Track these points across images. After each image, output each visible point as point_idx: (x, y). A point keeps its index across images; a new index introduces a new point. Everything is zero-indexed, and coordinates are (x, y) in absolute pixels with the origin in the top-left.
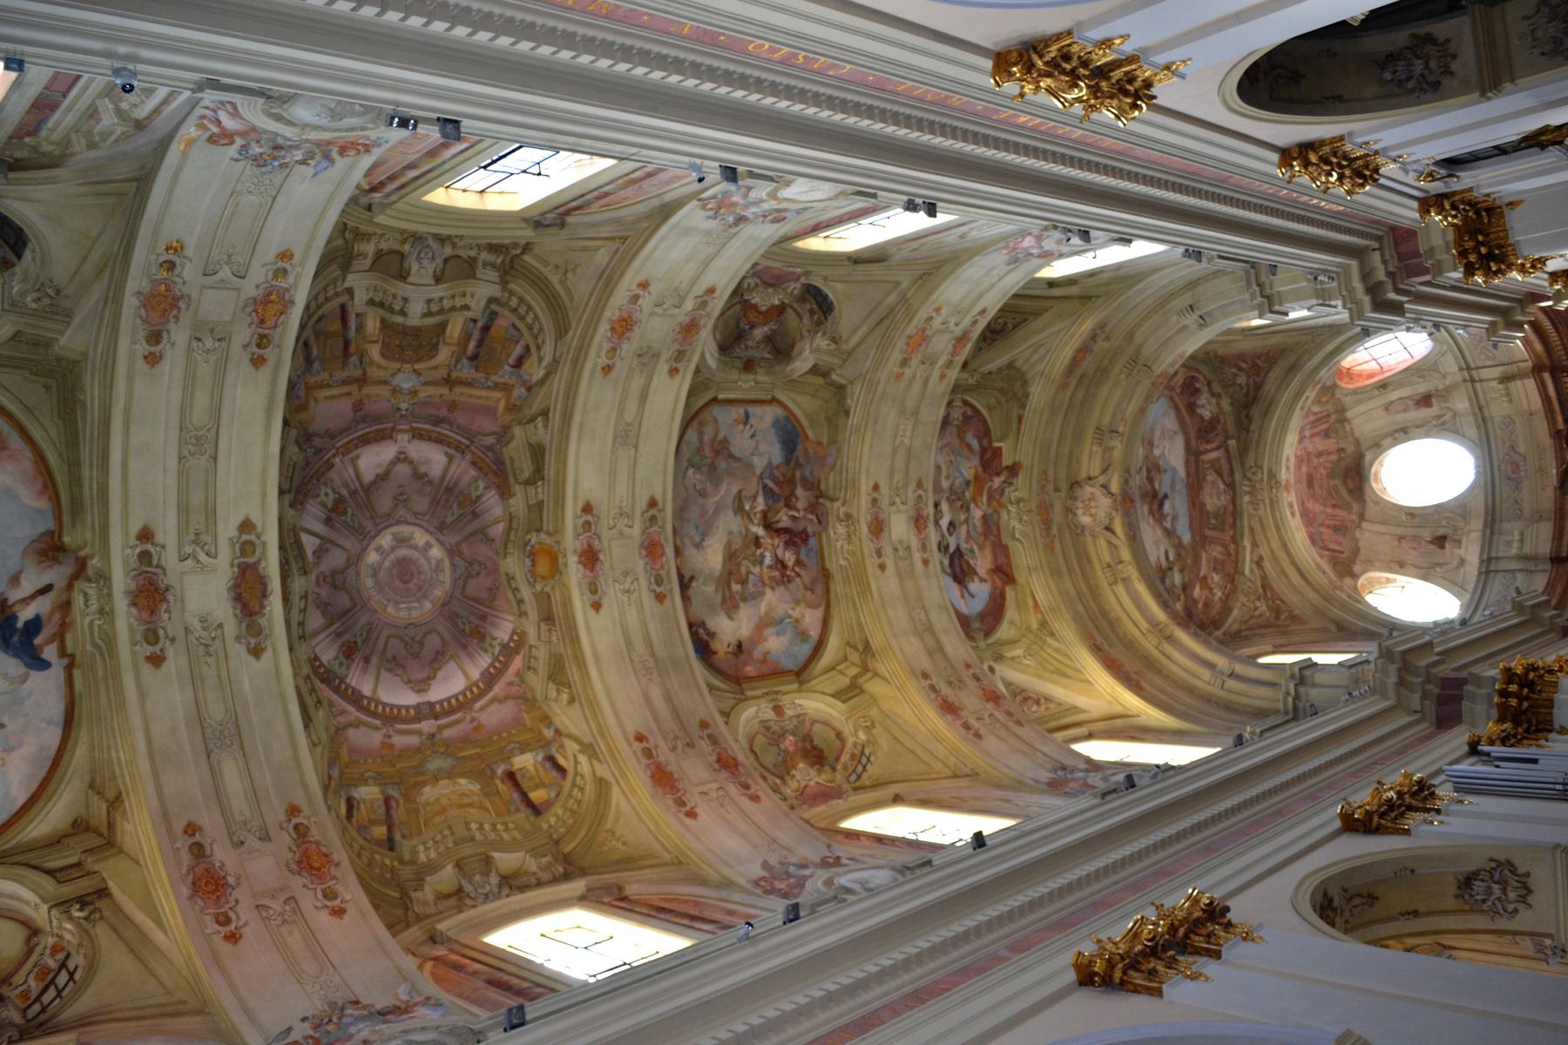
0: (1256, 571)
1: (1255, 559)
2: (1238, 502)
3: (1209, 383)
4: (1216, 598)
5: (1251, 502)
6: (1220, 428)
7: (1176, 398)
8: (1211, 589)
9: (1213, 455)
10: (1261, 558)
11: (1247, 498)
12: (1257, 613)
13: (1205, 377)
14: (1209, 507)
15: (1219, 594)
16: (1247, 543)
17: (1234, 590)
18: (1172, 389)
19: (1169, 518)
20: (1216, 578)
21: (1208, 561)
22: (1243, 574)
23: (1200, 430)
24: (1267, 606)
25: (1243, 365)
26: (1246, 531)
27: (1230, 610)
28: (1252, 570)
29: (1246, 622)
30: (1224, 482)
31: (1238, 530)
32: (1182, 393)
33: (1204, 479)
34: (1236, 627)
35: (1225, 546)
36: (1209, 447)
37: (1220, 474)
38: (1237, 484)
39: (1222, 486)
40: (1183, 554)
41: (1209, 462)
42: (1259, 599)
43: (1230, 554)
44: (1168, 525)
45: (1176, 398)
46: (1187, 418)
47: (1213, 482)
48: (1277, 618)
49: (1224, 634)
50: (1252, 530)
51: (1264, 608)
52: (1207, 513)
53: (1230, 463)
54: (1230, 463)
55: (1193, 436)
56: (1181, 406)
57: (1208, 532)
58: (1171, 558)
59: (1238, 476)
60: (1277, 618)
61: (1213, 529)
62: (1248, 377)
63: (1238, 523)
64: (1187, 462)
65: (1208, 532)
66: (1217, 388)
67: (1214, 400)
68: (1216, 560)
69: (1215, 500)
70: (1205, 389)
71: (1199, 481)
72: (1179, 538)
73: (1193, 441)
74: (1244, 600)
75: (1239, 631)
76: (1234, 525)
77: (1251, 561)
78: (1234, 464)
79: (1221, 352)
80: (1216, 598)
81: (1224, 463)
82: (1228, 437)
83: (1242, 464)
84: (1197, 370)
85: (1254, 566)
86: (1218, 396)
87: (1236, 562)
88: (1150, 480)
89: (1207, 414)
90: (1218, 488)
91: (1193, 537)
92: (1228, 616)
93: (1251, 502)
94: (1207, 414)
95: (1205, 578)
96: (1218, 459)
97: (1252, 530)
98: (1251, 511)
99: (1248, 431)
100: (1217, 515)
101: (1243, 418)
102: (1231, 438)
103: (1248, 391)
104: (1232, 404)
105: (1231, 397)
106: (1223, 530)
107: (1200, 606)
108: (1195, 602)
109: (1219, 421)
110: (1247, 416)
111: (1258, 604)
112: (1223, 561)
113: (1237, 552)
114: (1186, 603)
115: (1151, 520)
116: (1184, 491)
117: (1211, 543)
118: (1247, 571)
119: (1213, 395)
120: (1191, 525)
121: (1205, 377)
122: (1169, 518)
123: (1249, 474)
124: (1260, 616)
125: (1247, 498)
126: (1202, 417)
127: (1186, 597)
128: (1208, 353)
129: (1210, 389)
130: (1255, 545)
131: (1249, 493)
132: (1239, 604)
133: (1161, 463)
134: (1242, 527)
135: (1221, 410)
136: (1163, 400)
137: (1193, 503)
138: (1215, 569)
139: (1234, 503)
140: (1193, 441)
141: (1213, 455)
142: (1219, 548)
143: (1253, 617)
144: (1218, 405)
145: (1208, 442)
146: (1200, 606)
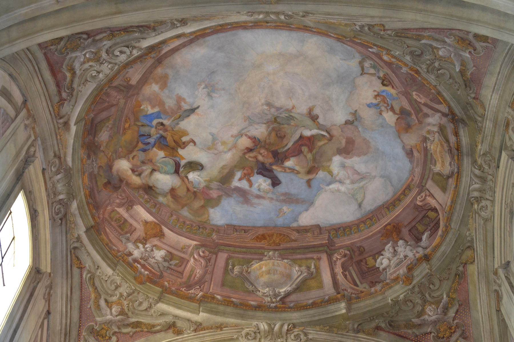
0: (161, 321)
1: (180, 324)
2: (259, 314)
3: (427, 258)
4: (130, 246)
5: (257, 331)
6: (363, 287)
7: (408, 200)
8: (144, 241)
9: (327, 278)
10: (179, 332)
11: (263, 326)
12: (102, 303)
13: (438, 246)
14: (256, 266)
15: (136, 254)
16: (202, 317)
17: (139, 280)
18: (422, 188)
19: (244, 184)
20: (159, 254)
21: (183, 249)
22: (160, 300)
23: (361, 250)
24: (110, 323)
25: (451, 313)
26: (219, 319)
27: (113, 266)
28: (163, 314)
29: (92, 279)
30: (288, 294)
31: (222, 308)
32: (417, 208)
33: (294, 261)
34: (88, 264)
35: (200, 282)
36: (339, 270)
37: (298, 289)
38: (285, 315)
39: (283, 290)
40: (197, 204)
41: (317, 268)
42: (122, 313)
43: (189, 287)
44: (236, 183)
45: (408, 200)
46: (378, 227)
47: (289, 276)
48: (92, 331)
49: (78, 239)
50: (220, 327)
51: (109, 317)
52: (248, 262)
53: (314, 305)
54: (314, 305)
55: (354, 239)
56: (398, 210)
57: (222, 257)
58: (192, 176)
59: (295, 316)
60: (92, 331)
61: (226, 270)
62: (435, 323)
63: (229, 309)
64: (317, 229)
65: (222, 257)
66: (423, 270)
67: (402, 271)
68: (183, 261)
69: (265, 279)
70: (421, 252)
71: (294, 250)
72: (215, 202)
73: (347, 241)
74: (124, 290)
75: (81, 268)
76: (228, 302)
77: (176, 316)
78: (312, 312)
79: (472, 269)
80: (130, 246)
81: (313, 295)
82: (349, 301)
83: (312, 324)
84: (444, 237)
85: (169, 319)
86: (408, 278)
87: (177, 294)
88: (296, 151)
89: (383, 262)
90: (281, 285)
91: (217, 229)
92: (105, 257)
93: (257, 331)
94: (383, 262)
95: (161, 235)
96: (321, 286)
97: (220, 327)
98: (246, 330)
99: (357, 331)
100: (244, 277)
101: (373, 325)
102: (349, 308)
103: (414, 326)
104: (396, 302)
105: (406, 300)
106: (223, 285)
107: (122, 211)
108: (129, 205)
109: (373, 284)
110: (378, 328)
111: (115, 309)
112: (182, 273)
113: (191, 299)
114: (128, 184)
115: (245, 142)
116: (280, 221)
117: (208, 260)
118: (162, 306)
119: (410, 269)
120: (235, 228)
121: (438, 246)
122: (244, 184)
123: (296, 331)
124: (98, 307)
125: (263, 326)
126: (380, 253)
127: (138, 188)
128: (471, 247)
129: (419, 260)
130: (198, 327)
131: (271, 329)
132: (118, 280)
133: (321, 174)
134: (224, 314)
135: (388, 286)
136: (405, 164)
137: (263, 237)
138: (170, 257)
139: (259, 307)
140: (347, 241)
141: (327, 278)
142: (199, 272)
143: (98, 296)
144: (396, 280)
145: (344, 267)
146: (122, 211)
